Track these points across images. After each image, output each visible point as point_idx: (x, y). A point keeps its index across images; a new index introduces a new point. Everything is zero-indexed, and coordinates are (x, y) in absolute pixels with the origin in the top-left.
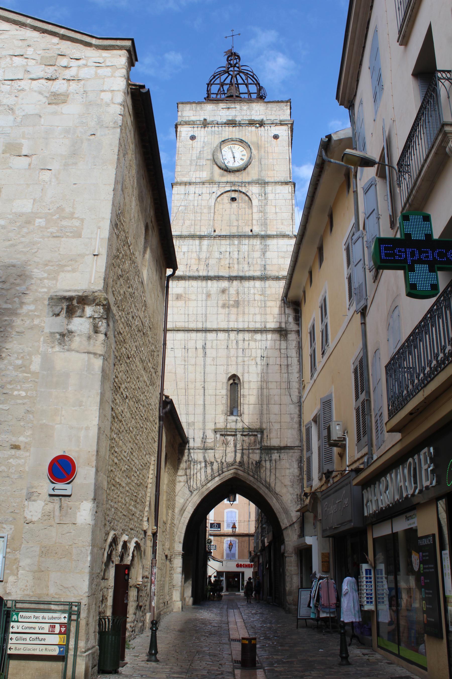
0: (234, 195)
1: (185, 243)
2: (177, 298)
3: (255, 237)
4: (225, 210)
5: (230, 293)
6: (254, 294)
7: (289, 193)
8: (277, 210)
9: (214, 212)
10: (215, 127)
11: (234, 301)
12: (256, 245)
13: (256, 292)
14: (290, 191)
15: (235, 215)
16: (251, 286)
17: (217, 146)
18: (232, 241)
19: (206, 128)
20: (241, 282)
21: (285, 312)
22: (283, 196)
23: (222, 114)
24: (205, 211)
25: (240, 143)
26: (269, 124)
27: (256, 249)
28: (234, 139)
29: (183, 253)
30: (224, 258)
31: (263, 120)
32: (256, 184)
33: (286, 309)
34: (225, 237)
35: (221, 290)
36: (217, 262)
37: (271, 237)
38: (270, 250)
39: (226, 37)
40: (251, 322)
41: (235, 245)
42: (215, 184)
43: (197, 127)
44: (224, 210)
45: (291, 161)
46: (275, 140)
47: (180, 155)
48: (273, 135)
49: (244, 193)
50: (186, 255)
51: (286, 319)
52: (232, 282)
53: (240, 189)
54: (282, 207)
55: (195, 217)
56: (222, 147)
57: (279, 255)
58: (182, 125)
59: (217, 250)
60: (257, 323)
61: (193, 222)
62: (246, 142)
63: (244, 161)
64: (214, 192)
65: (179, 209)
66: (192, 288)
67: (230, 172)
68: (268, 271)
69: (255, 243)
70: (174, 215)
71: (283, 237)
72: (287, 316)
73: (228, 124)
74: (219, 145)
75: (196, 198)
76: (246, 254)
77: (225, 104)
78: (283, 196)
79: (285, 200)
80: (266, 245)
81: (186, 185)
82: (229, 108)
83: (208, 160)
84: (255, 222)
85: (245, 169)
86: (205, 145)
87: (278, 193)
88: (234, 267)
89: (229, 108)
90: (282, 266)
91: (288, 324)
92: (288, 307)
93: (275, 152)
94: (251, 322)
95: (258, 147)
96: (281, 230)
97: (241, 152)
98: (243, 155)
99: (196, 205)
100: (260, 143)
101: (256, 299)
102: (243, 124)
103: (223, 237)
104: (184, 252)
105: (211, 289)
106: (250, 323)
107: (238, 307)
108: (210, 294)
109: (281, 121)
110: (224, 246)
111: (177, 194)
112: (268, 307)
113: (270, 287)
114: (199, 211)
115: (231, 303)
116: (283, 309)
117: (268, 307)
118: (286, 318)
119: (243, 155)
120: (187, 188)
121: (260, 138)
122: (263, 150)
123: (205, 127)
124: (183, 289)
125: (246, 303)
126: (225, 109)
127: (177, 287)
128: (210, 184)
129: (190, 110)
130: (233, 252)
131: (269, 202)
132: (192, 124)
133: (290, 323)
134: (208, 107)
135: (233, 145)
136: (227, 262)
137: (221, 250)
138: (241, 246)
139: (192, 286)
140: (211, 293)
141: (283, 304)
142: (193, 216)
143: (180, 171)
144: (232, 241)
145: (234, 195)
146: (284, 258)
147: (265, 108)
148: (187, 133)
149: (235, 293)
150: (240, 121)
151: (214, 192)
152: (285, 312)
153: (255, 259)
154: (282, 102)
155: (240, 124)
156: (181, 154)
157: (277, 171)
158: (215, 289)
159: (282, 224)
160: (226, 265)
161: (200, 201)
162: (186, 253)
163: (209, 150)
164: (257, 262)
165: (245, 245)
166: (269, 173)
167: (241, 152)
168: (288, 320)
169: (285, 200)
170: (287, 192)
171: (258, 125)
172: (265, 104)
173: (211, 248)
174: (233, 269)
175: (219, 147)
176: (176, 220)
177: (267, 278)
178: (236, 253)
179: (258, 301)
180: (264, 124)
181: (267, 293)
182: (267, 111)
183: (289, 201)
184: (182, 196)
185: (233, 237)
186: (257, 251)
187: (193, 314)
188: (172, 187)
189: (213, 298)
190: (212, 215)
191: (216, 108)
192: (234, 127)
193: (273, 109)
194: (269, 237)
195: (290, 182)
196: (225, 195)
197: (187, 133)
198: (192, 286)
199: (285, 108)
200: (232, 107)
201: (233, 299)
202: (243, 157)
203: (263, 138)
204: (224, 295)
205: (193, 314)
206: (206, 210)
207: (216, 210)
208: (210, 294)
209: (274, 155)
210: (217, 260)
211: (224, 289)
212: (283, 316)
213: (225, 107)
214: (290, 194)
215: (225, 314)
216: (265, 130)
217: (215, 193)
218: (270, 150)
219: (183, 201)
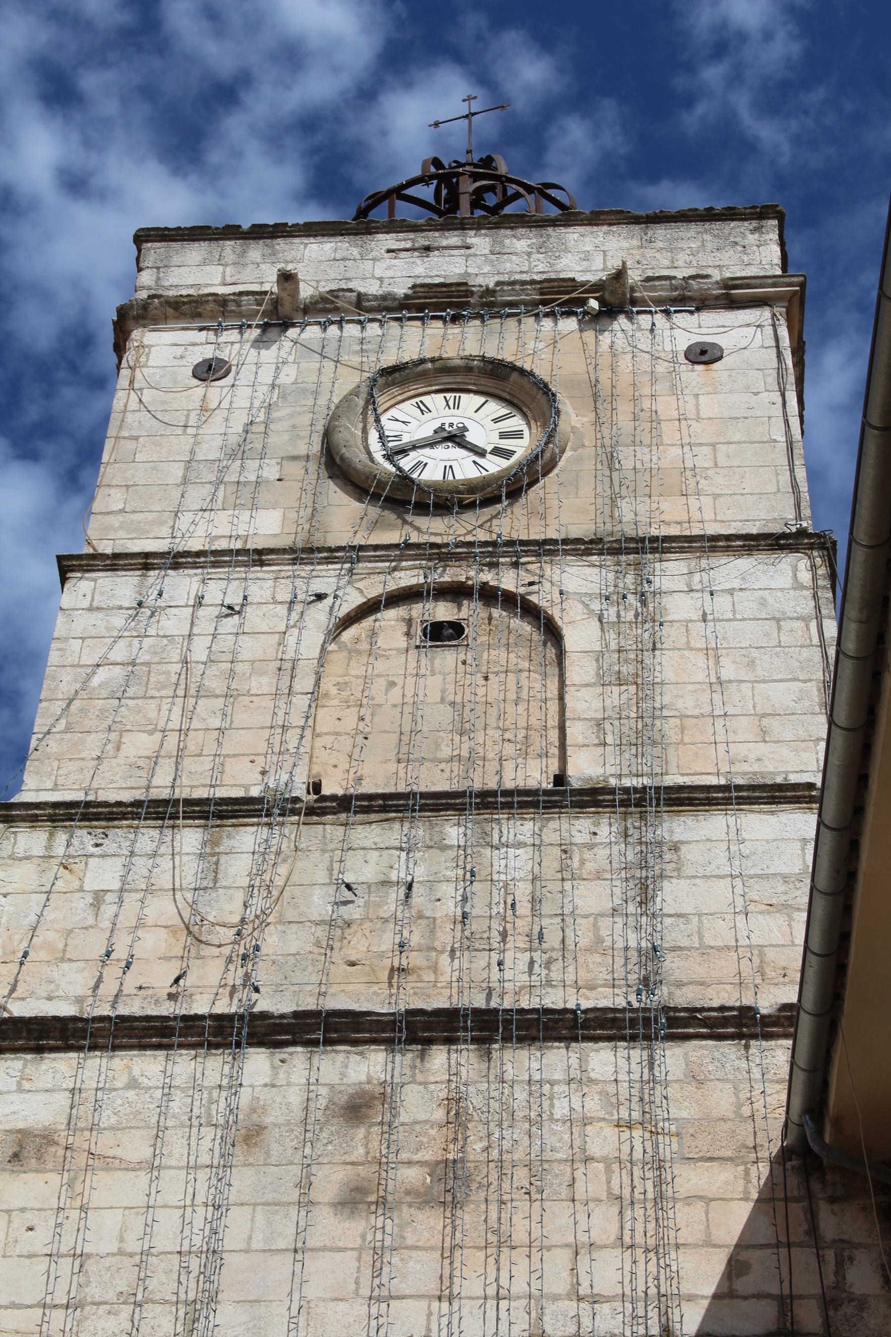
0: (443, 611)
1: (110, 846)
2: (16, 1156)
3: (582, 805)
4: (392, 684)
5: (404, 1117)
6: (586, 1121)
7: (798, 586)
8: (728, 671)
9: (316, 695)
10: (340, 323)
11: (432, 1167)
12: (591, 847)
13: (593, 1105)
14: (805, 577)
15: (453, 704)
16: (559, 1075)
17: (355, 392)
18: (432, 827)
19: (292, 332)
20: (488, 1055)
21: (813, 1230)
22: (763, 603)
23: (390, 273)
24: (264, 683)
25: (488, 383)
26: (658, 302)
27: (590, 866)
28: (458, 362)
29: (89, 899)
30: (367, 918)
31: (620, 275)
32: (588, 553)
33: (824, 1211)
34: (384, 809)
35: (343, 1100)
36: (318, 944)
37: (691, 802)
38: (688, 871)
39: (437, 124)
40: (556, 1298)
41: (444, 848)
42: (328, 561)
43: (241, 327)
44: (381, 683)
45: (799, 451)
46: (700, 368)
47: (131, 445)
48: (683, 346)
49: (509, 600)
50: (108, 911)
51: (830, 1278)
52: (422, 1056)
53: (488, 577)
54: (755, 653)
55: (188, 714)
56: (382, 400)
57: (753, 895)
58: (156, 320)
59: (321, 876)
60: (604, 1309)
61: (172, 741)
62: (522, 371)
63: (514, 459)
64: (320, 597)
65: (89, 677)
66: (131, 1094)
67: (422, 509)
68: (680, 984)
69: (579, 839)
70: (57, 707)
71: (772, 801)
72: (830, 1255)
73: (420, 308)
74: (364, 390)
75: (205, 626)
76: (523, 891)
77: (411, 235)
78: (763, 603)
79: (778, 621)
80: (660, 844)
81: (147, 567)
82: (428, 249)
83: (295, 458)
84: (576, 732)
85: (515, 494)
86: (283, 396)
87: (731, 592)
88: (435, 968)
89: (428, 249)
90: (771, 954)
91: (848, 1309)
92: (832, 1200)
93: (698, 419)
94: (556, 1298)
95: (595, 397)
96: (756, 768)
97: (496, 421)
98: (503, 435)
99: (199, 652)
100: (604, 377)
101: (594, 1149)
102: (511, 304)
103: (367, 810)
104: (99, 897)
105: (265, 1095)
106: (551, 1308)
107: (455, 1204)
108: (260, 1129)
109: (729, 284)
110: (375, 854)
111: (90, 609)
112: (689, 1199)
113: (696, 1079)
114: (215, 682)
115: (413, 1176)
116: (797, 1210)
117: (689, 1199)
118: (830, 1267)
119: (503, 435)
120: (151, 580)
121: (605, 361)
122: (624, 411)
123: (286, 325)
124: (62, 1100)
125: (521, 1176)
126: (403, 254)
127: (20, 1090)
128: (294, 562)
129: (204, 263)
130: (431, 884)
131: (671, 635)
132: (213, 318)
133: (862, 1303)
134: (314, 246)
135: (448, 395)
136: (387, 941)
137: (349, 878)
138: (488, 851)
139: (133, 1084)
140: (268, 1120)
141: (793, 1181)
142: (177, 711)
143: (122, 511)
144: (432, 827)
145: (443, 611)
146: (786, 908)
147: (635, 242)
148: (180, 351)
149: (439, 1115)
150: (489, 292)
151: (320, 597)
152: (813, 1230)
153: (584, 924)
154: (730, 215)
155: (490, 305)
156: (136, 438)
157: (716, 496)
158: (295, 1097)
159: (764, 736)
160: (381, 955)
161: (226, 643)
162: (109, 897)
163: (306, 419)
164: (599, 940)
165: (520, 845)
166: (664, 506)
167: (496, 421)
168: (840, 1284)
169: (778, 621)
170: (785, 581)
171: (594, 304)
172: (636, 228)
173: (283, 870)
174: (429, 976)
175: (364, 395)
176: (68, 730)
177: (673, 1022)
178: (449, 893)
179: (605, 1159)
180: (634, 302)
181: (674, 1113)
182: (649, 253)
183: (801, 624)
184: (118, 621)
185: (436, 809)
186: (598, 876)
187: (121, 1252)
188: (64, 580)
189: (275, 1148)
190: (301, 702)
191: (355, 252)
192: (455, 319)
193: (683, 244)
194: (680, 802)
195: (802, 533)
196: (391, 616)
197: (180, 351)
198: (133, 1084)
199: (752, 238)
200: (445, 243)
201: (427, 1155)
202: (506, 444)
203: (625, 364)
204: (361, 1132)
205: (121, 1252)
206: (265, 680)
207: (327, 685)
208: (260, 1129)
209: (696, 427)
210: (321, 932)
211: (362, 1094)
212: (804, 1257)
213: (409, 245)
214: (808, 593)
215: (360, 1249)
216: (640, 329)
217: (329, 601)
218: (666, 406)
219: (122, 643)
